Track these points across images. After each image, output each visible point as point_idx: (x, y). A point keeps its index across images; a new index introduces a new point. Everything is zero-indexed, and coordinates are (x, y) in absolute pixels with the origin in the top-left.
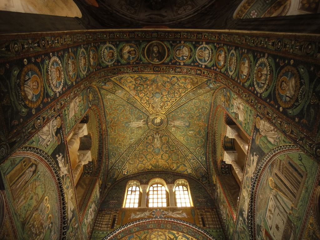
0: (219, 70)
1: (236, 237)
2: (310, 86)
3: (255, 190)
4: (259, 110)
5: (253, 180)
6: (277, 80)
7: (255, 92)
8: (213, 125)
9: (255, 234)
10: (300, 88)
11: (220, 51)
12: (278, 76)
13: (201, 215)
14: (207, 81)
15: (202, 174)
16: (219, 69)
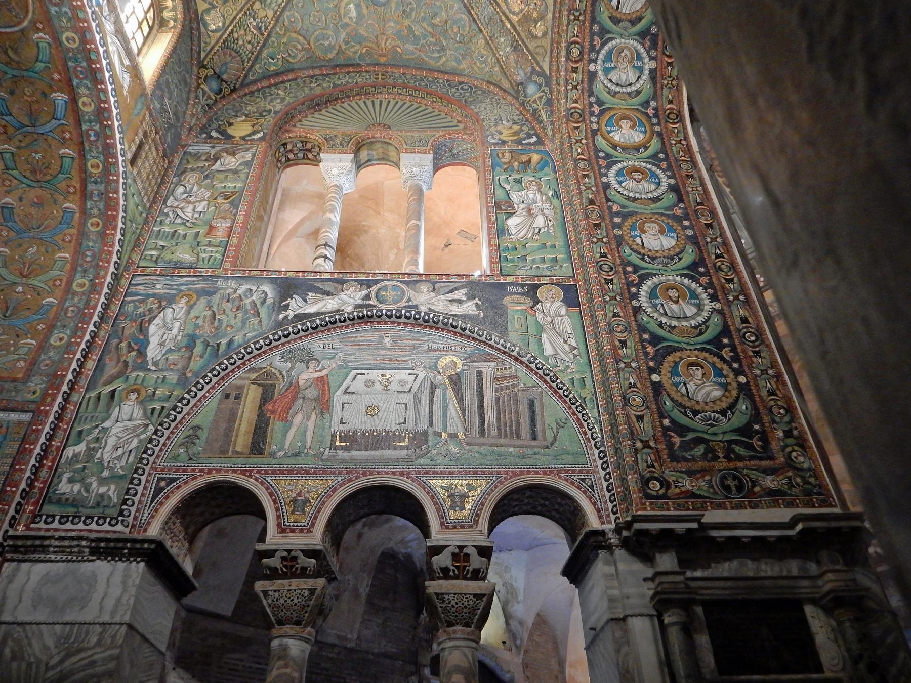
0: (595, 126)
1: (193, 283)
2: (731, 431)
3: (388, 320)
4: (611, 314)
5: (413, 313)
6: (695, 350)
7: (634, 290)
8: (394, 87)
9: (277, 347)
10: (717, 412)
11: (641, 124)
12: (702, 350)
13: (145, 134)
14: (542, 74)
15: (225, 72)
16: (598, 123)
